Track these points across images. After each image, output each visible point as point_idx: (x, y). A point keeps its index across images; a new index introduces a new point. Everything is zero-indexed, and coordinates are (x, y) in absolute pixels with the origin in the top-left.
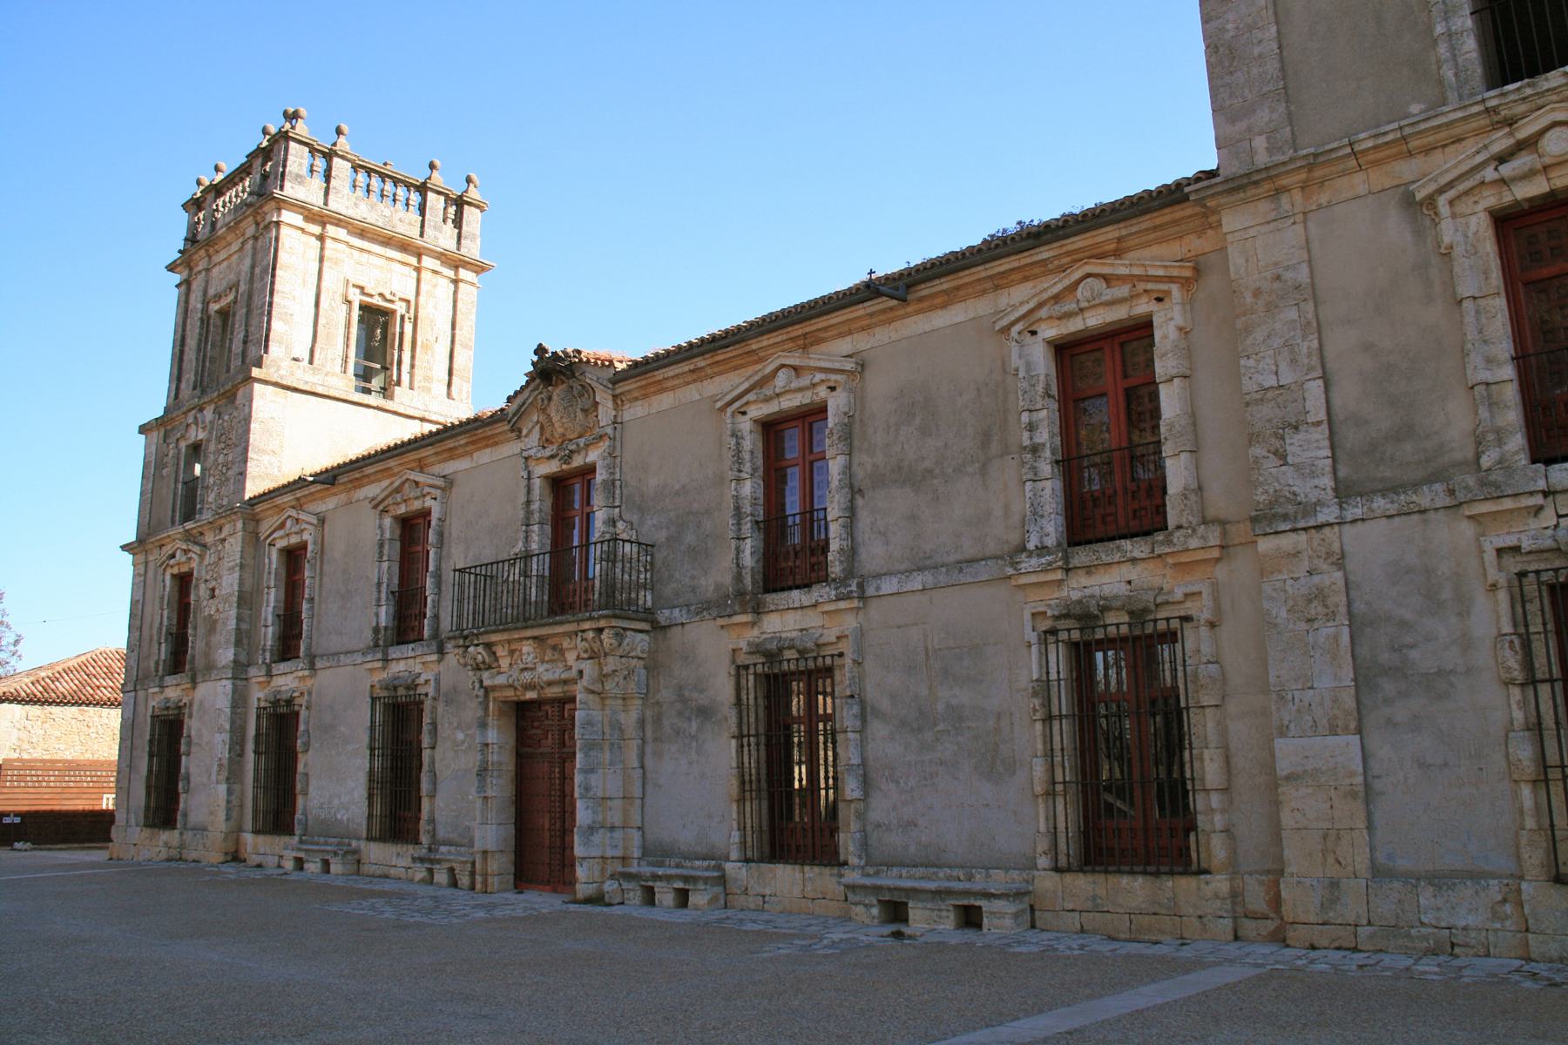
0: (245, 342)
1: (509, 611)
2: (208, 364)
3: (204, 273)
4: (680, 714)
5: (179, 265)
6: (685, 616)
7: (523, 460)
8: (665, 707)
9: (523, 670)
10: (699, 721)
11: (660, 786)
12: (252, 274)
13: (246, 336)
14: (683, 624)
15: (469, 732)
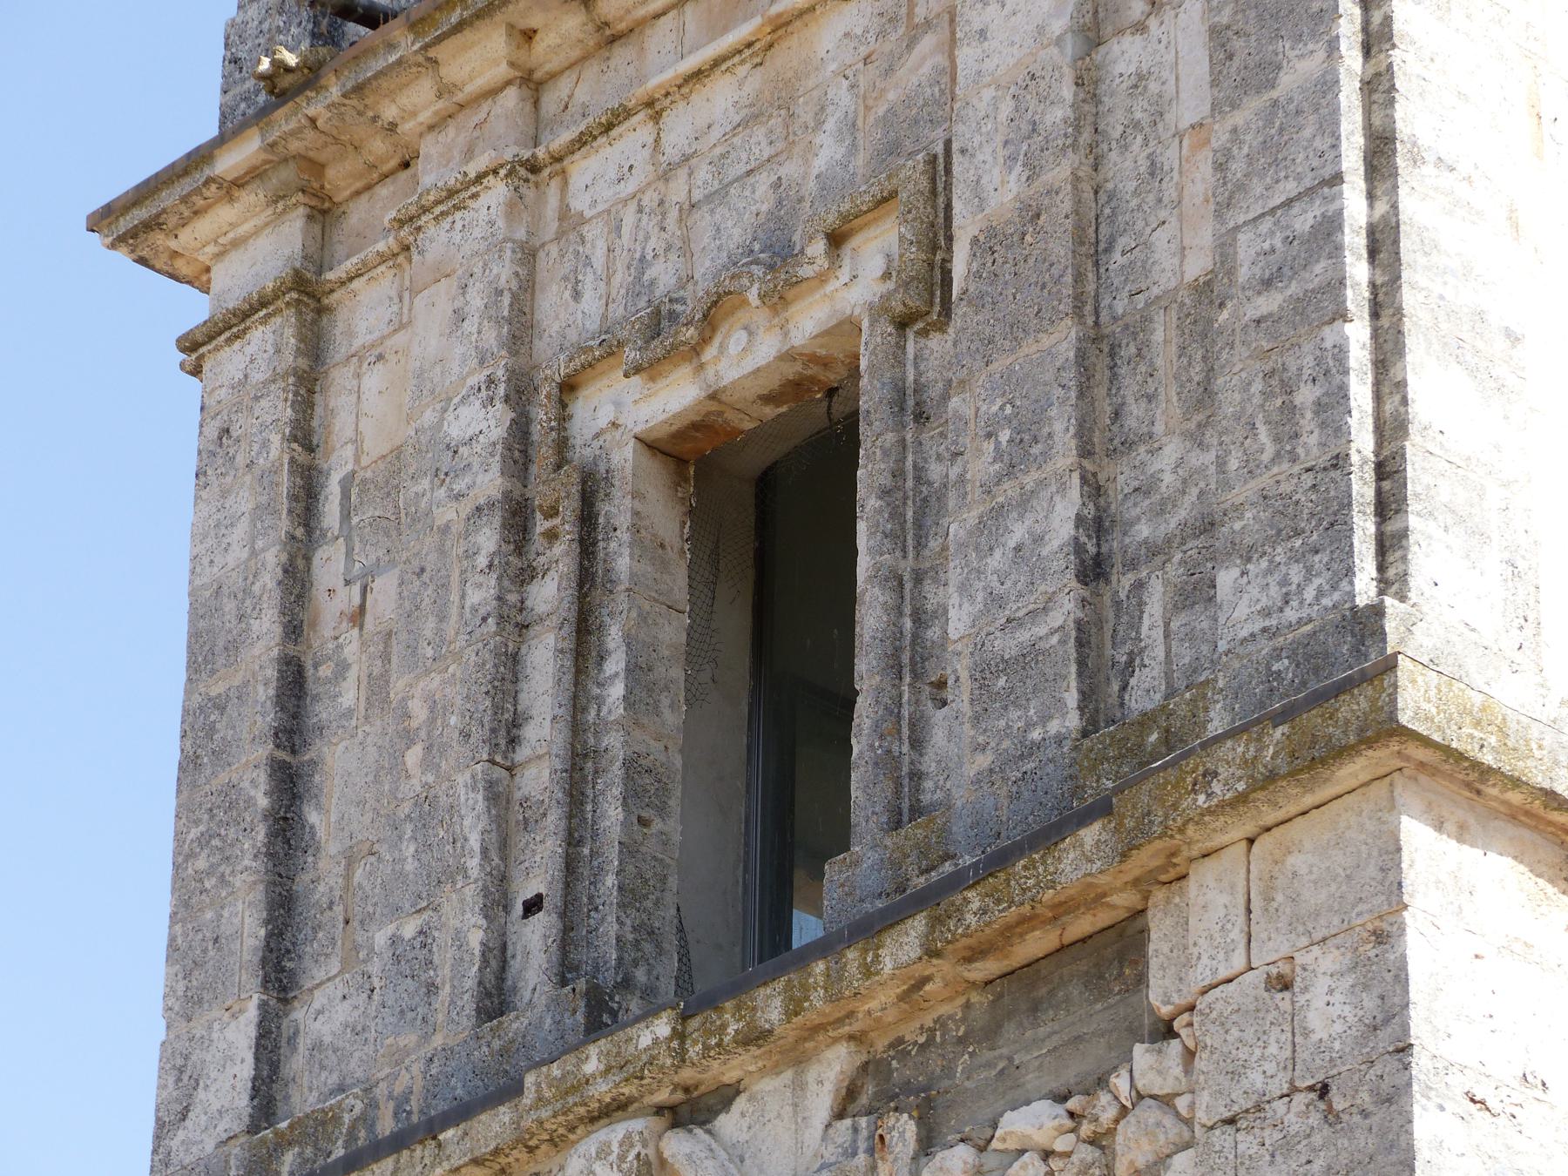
0: (1093, 570)
2: (612, 815)
3: (497, 192)
5: (232, 187)
12: (1088, 84)
13: (1097, 523)
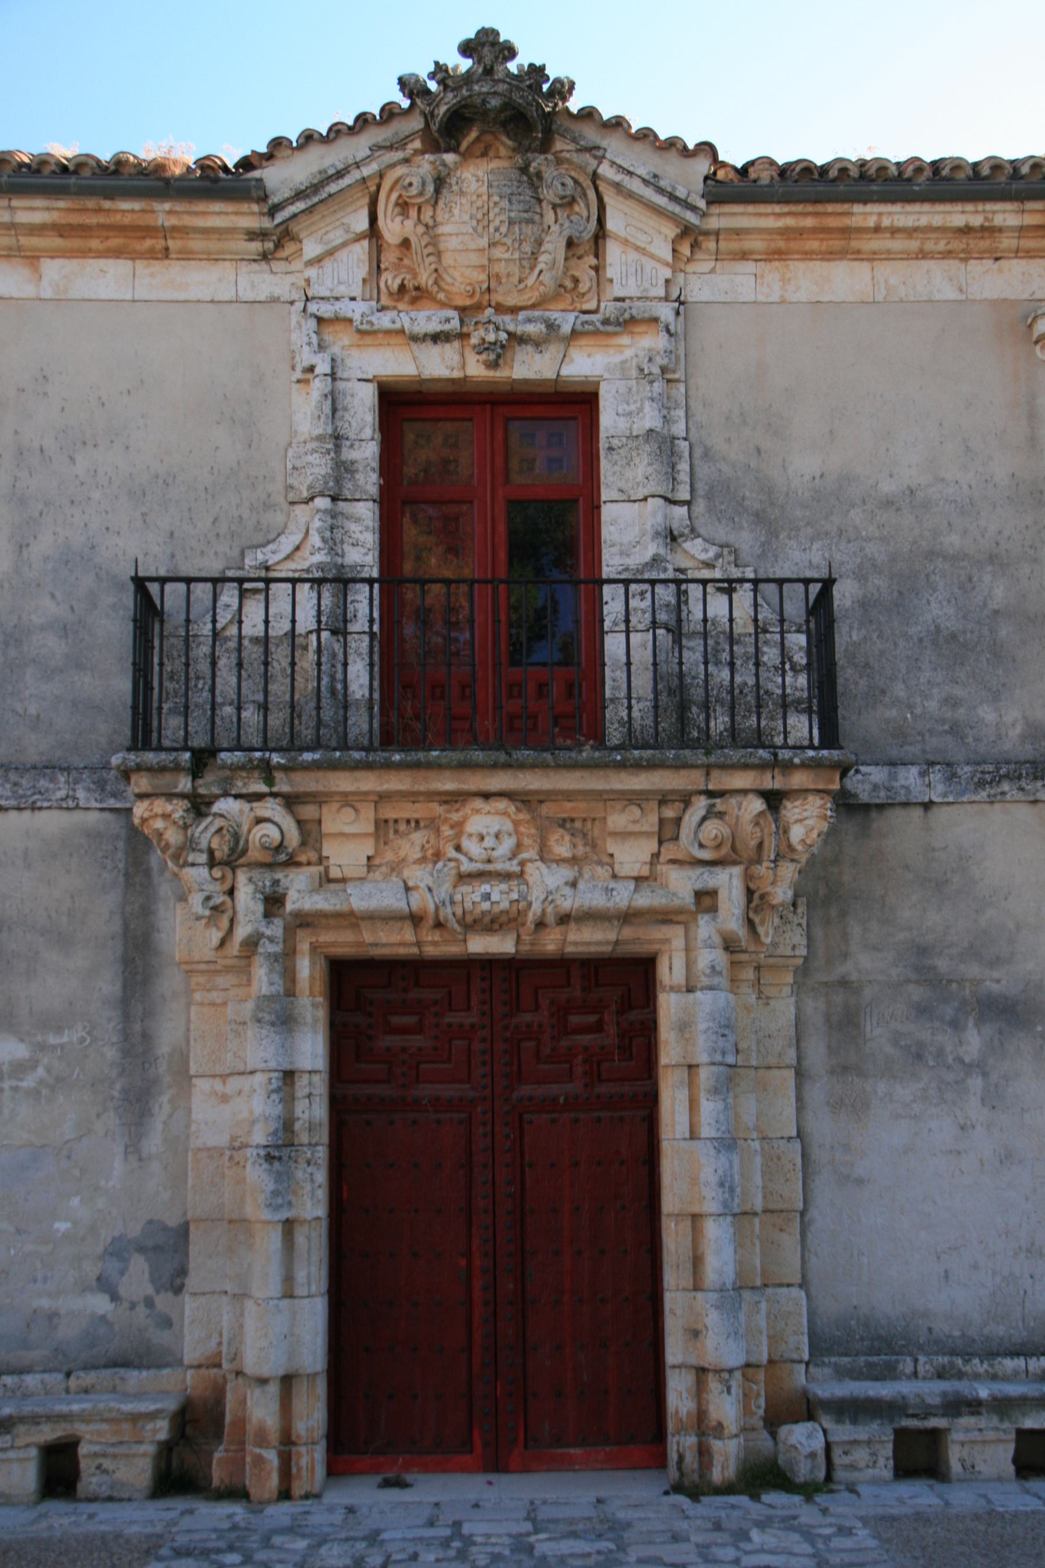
1: (250, 714)
4: (923, 1011)
6: (940, 788)
7: (312, 324)
8: (868, 993)
9: (463, 878)
10: (988, 1029)
11: (860, 1182)
14: (927, 806)
15: (53, 1039)
